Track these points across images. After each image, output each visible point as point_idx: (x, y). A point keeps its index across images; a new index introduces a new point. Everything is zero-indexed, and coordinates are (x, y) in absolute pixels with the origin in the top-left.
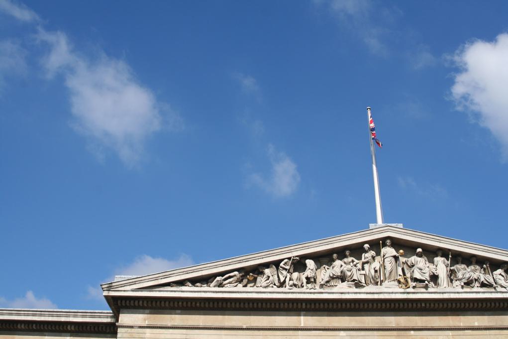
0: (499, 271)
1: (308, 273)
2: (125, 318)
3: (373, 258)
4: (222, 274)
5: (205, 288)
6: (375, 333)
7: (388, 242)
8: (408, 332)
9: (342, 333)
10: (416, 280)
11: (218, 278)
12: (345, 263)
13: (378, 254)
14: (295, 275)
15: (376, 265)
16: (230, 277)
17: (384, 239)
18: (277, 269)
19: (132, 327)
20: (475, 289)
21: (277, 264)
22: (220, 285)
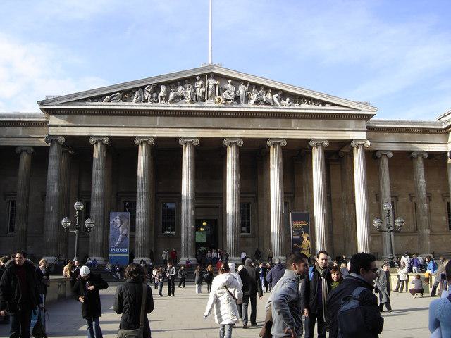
0: (277, 95)
1: (161, 94)
2: (54, 120)
3: (202, 87)
4: (110, 94)
5: (99, 103)
6: (200, 130)
7: (211, 75)
8: (219, 130)
9: (181, 130)
10: (226, 99)
11: (108, 97)
12: (186, 88)
13: (205, 82)
14: (155, 95)
15: (203, 90)
16: (115, 96)
17: (209, 74)
18: (144, 91)
19: (57, 126)
20: (261, 106)
21: (143, 88)
22: (109, 101)
